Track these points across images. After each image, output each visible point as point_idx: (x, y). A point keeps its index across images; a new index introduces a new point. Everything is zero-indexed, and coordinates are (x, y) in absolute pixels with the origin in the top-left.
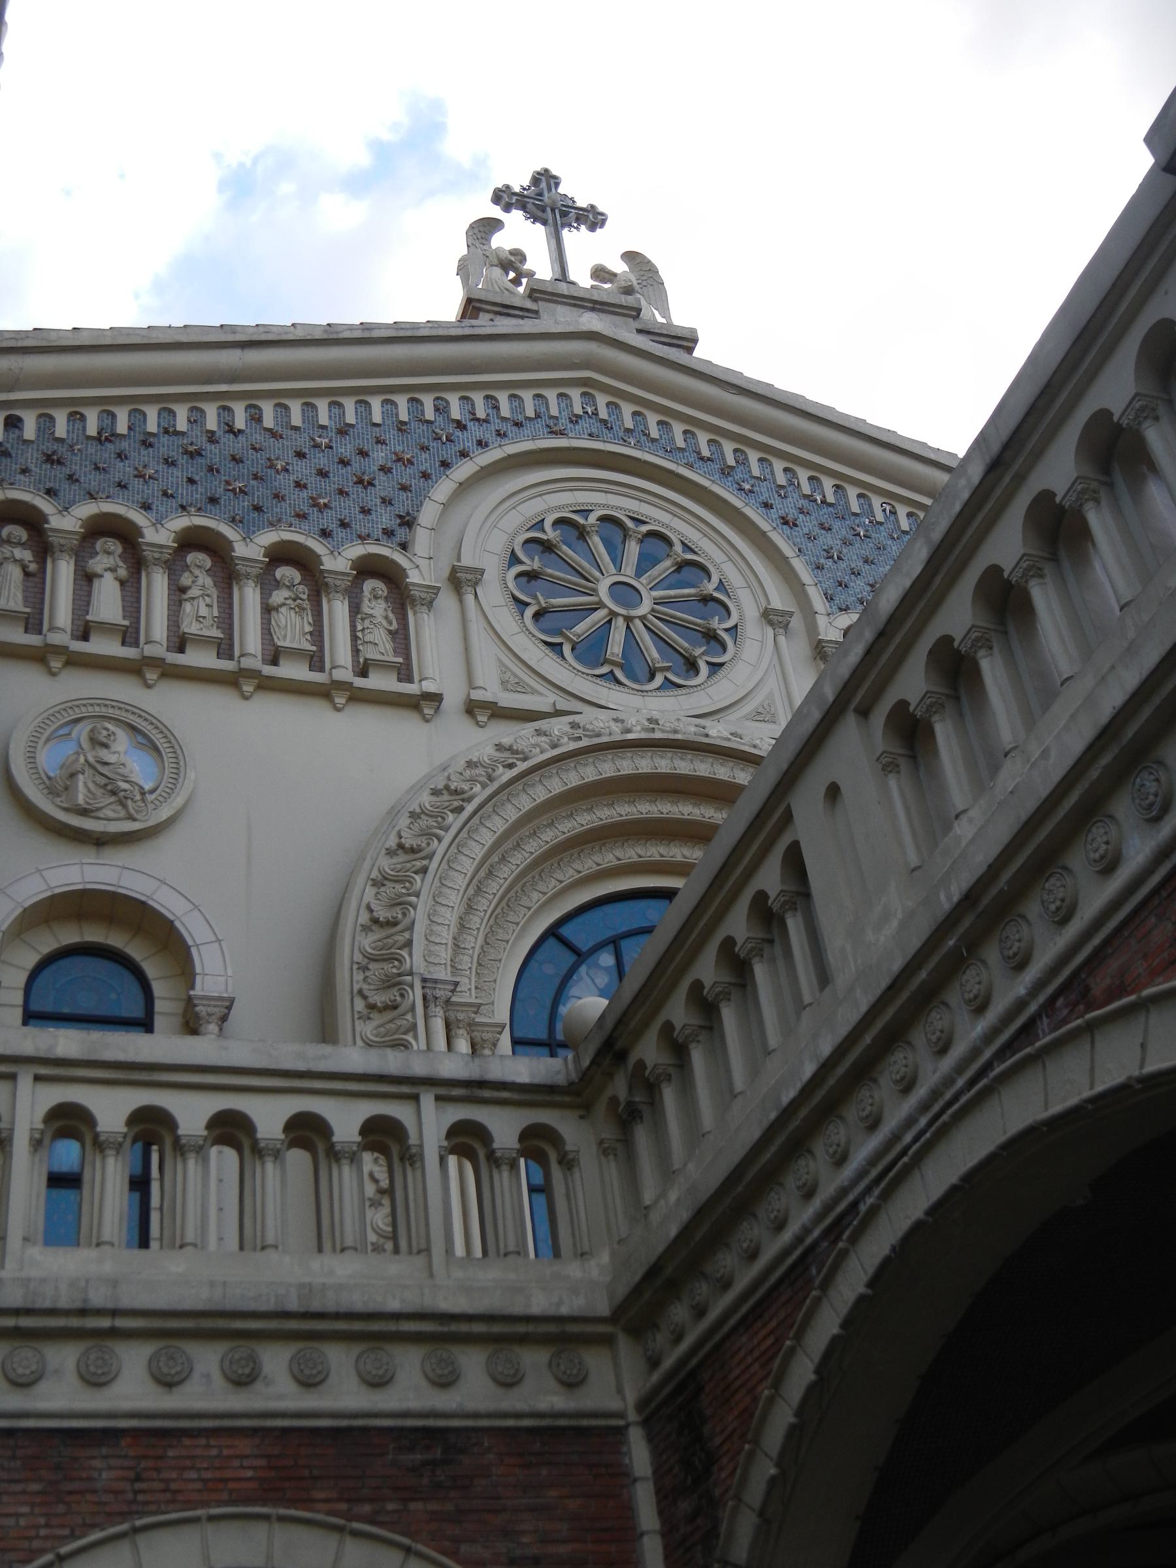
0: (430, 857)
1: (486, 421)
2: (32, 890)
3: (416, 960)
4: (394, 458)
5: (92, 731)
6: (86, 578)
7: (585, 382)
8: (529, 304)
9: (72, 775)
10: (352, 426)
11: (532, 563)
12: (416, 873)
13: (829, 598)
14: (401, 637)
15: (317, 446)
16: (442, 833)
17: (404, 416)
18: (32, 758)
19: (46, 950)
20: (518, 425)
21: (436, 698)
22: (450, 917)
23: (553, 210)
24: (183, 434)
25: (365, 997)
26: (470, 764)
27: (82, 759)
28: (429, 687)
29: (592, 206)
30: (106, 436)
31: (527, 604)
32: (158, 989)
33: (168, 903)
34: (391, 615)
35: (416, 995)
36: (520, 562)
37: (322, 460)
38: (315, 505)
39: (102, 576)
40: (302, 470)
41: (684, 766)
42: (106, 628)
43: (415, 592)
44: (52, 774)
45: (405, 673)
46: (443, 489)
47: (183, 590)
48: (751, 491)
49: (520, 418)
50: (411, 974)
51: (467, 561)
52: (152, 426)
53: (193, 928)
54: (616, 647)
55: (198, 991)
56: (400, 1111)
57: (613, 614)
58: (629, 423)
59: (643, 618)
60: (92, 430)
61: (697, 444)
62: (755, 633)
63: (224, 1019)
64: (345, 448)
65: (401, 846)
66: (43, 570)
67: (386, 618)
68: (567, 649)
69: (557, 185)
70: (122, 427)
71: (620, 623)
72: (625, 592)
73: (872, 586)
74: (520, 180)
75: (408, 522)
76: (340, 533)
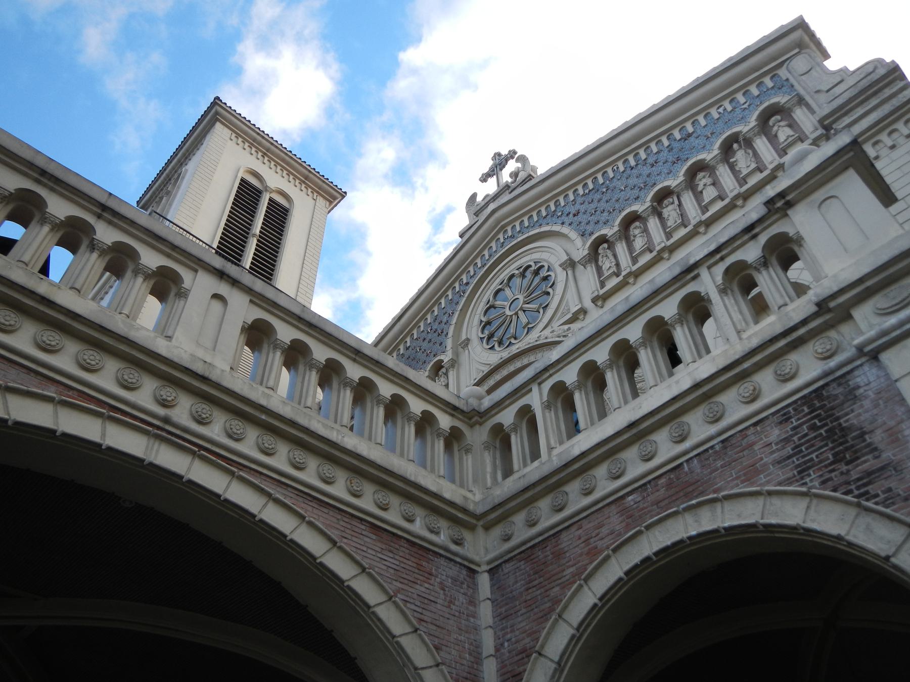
59: (521, 309)
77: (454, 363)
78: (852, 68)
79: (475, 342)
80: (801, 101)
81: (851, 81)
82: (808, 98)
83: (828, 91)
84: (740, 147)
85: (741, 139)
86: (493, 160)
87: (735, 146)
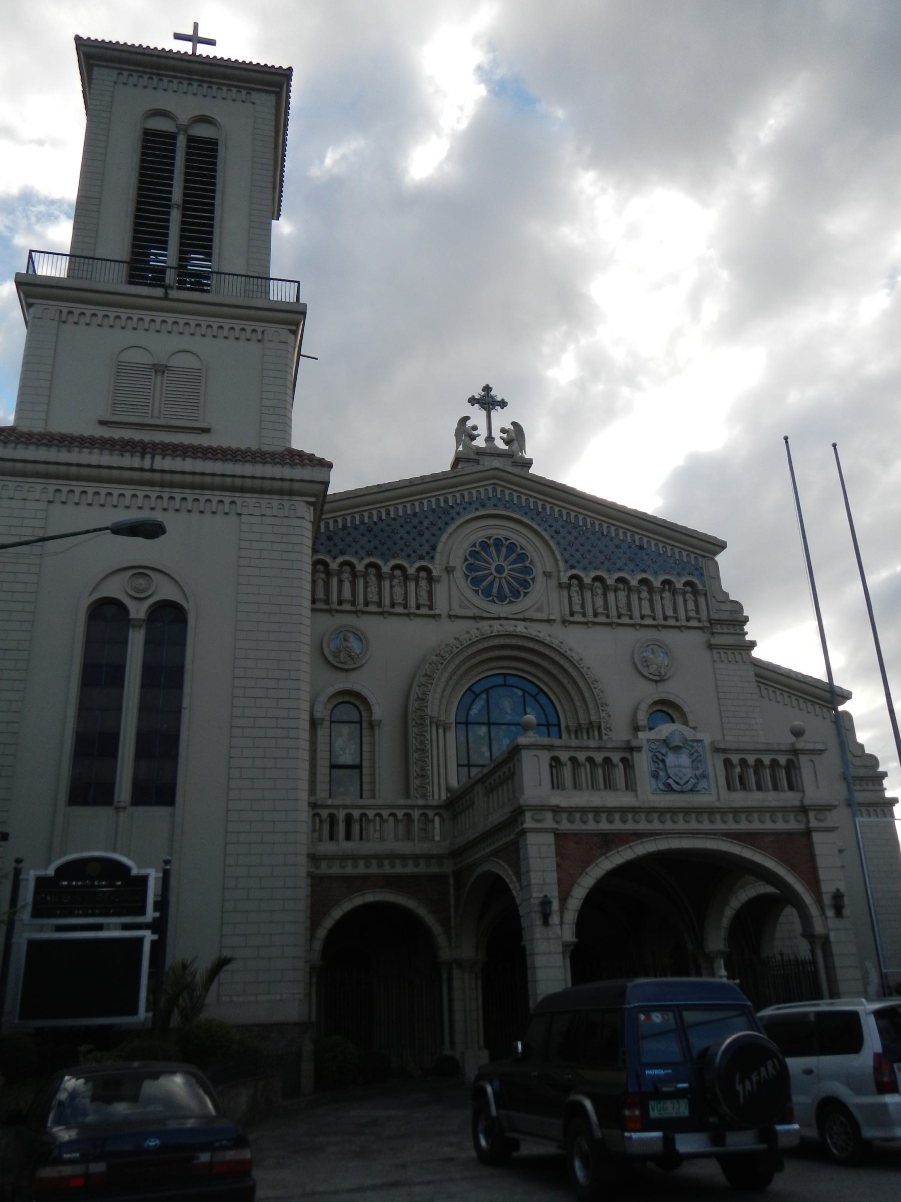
0: (434, 679)
1: (460, 504)
2: (331, 691)
3: (429, 711)
4: (431, 523)
5: (344, 635)
6: (341, 582)
7: (494, 484)
8: (476, 457)
9: (339, 652)
10: (417, 513)
11: (471, 561)
12: (429, 684)
13: (566, 562)
14: (430, 593)
15: (407, 522)
16: (437, 671)
17: (434, 506)
18: (329, 647)
19: (335, 704)
20: (470, 503)
21: (439, 615)
22: (437, 702)
23: (488, 404)
24: (366, 523)
25: (415, 721)
26: (447, 645)
27: (342, 647)
28: (437, 612)
29: (503, 400)
30: (345, 527)
31: (469, 576)
32: (363, 714)
33: (366, 693)
34: (427, 585)
35: (428, 722)
36: (468, 560)
37: (408, 527)
38: (406, 545)
39: (344, 581)
40: (402, 532)
41: (508, 641)
42: (346, 601)
43: (434, 578)
44: (334, 650)
45: (431, 607)
46: (444, 538)
47: (368, 583)
48: (546, 521)
49: (471, 501)
50: (426, 715)
51: (451, 564)
52: (358, 522)
53: (372, 699)
54: (495, 590)
55: (372, 719)
56: (410, 811)
57: (495, 577)
58: (507, 499)
59: (505, 578)
60: (340, 526)
61: (529, 504)
62: (540, 579)
63: (379, 726)
64: (415, 521)
65: (426, 674)
66: (328, 580)
67: (426, 586)
68: (480, 592)
69: (491, 391)
70: (349, 524)
71: (497, 580)
72: (499, 569)
73: (582, 555)
74: (478, 393)
75: (434, 548)
76: (413, 555)
77: (439, 580)
78: (731, 598)
79: (459, 574)
80: (706, 595)
81: (727, 607)
82: (708, 596)
83: (718, 602)
84: (669, 590)
85: (672, 586)
86: (483, 390)
87: (667, 587)
